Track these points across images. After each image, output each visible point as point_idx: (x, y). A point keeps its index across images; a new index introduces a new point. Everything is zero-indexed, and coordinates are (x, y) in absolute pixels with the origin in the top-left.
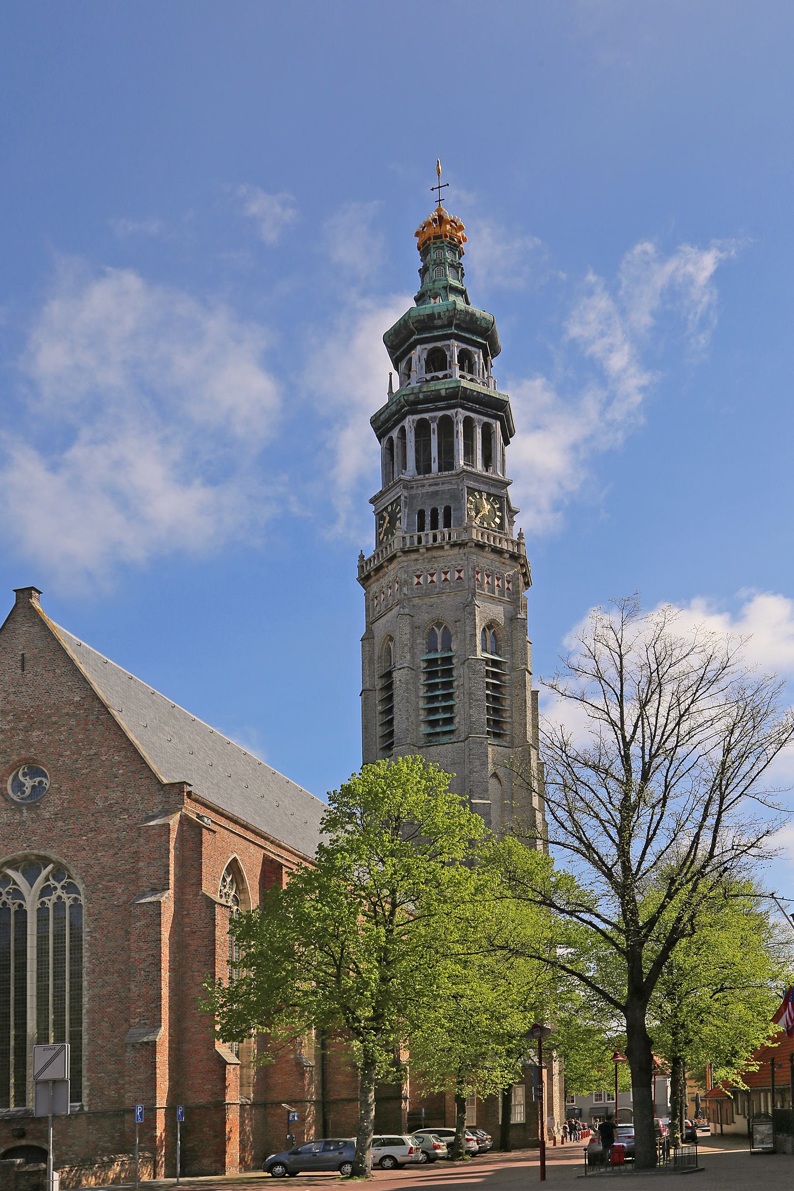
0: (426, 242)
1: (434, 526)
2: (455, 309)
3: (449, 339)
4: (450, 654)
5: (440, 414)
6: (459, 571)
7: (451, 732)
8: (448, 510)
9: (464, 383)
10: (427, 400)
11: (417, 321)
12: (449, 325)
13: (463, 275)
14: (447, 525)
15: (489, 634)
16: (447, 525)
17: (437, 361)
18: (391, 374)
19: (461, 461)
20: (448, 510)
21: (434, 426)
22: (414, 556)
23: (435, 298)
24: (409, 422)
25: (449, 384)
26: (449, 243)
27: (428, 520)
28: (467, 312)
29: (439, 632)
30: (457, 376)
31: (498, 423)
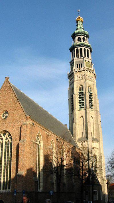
1: (80, 67)
4: (83, 91)
8: (82, 64)
9: (83, 43)
10: (78, 45)
12: (81, 33)
14: (82, 67)
16: (82, 67)
17: (79, 39)
24: (76, 49)
27: (78, 66)
29: (81, 87)
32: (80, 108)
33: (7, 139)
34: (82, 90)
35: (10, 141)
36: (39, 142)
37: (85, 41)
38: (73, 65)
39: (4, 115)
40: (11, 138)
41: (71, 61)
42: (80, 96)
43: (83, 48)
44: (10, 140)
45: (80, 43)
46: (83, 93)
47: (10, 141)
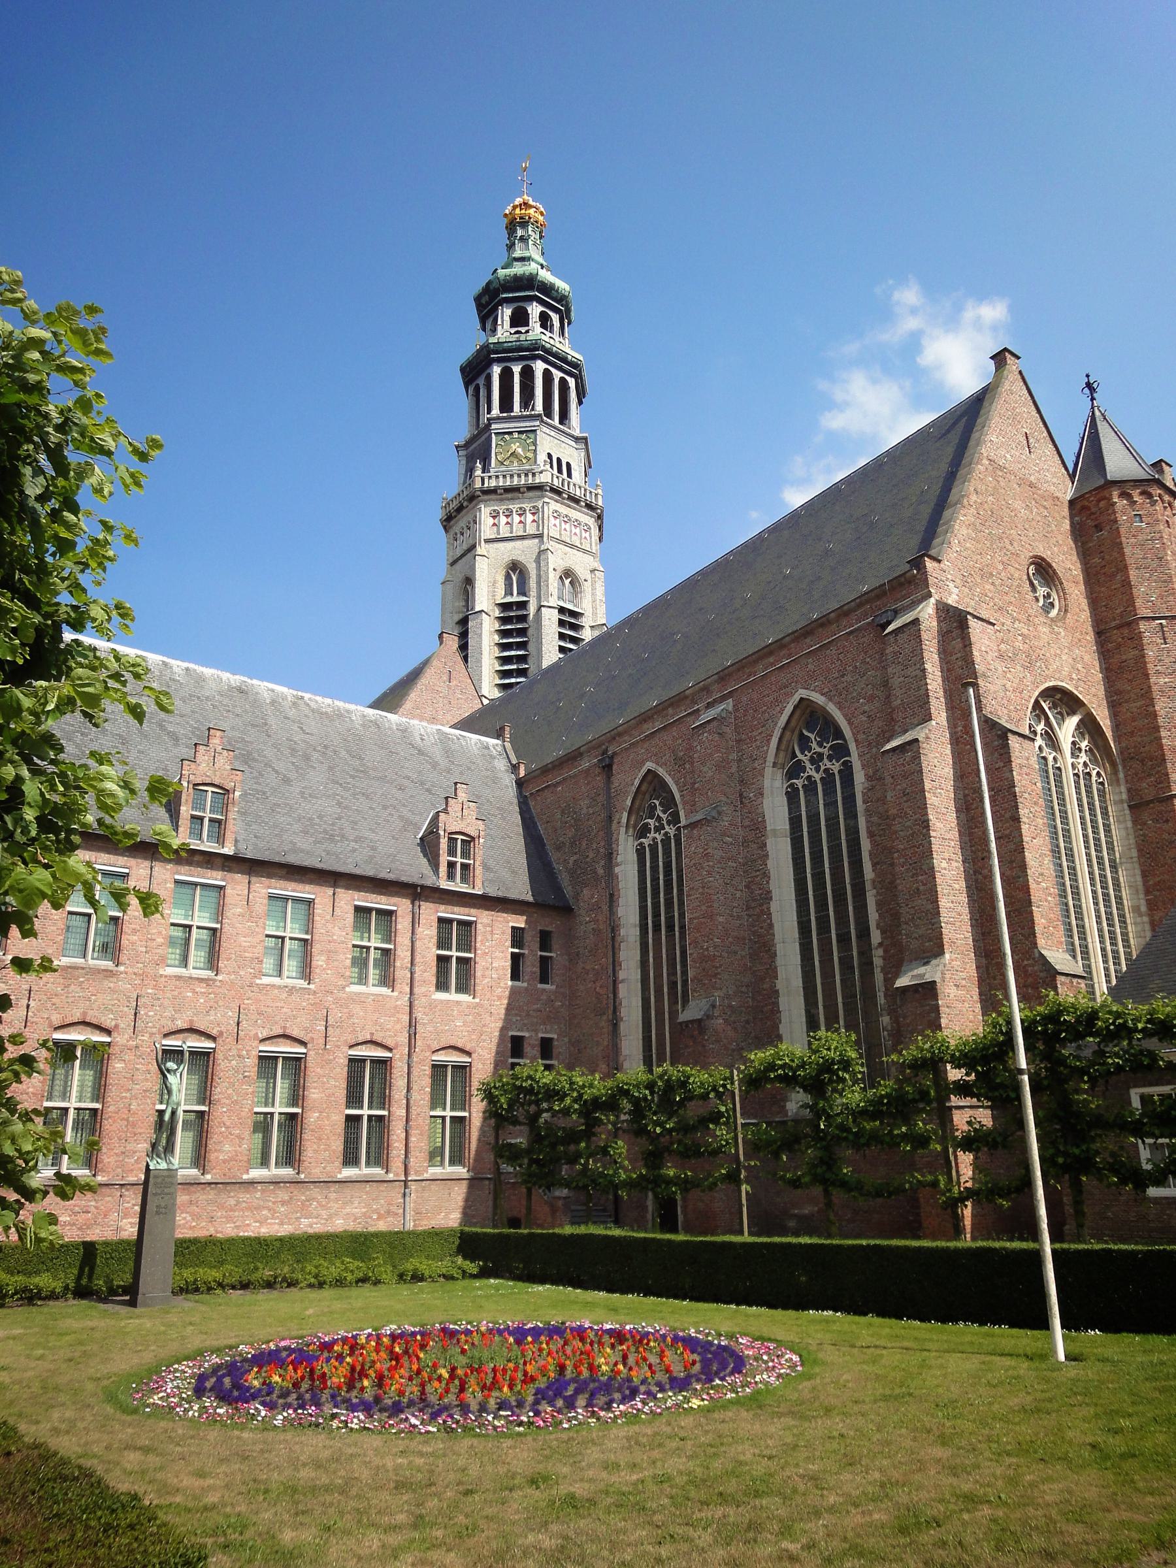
12: (531, 288)
15: (567, 582)
17: (519, 319)
24: (496, 370)
42: (504, 620)
46: (523, 605)
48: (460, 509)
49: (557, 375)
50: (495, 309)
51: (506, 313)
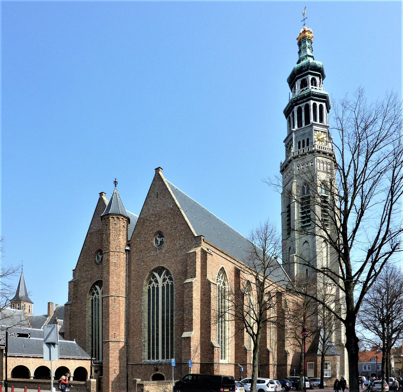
0: (300, 41)
1: (303, 146)
2: (309, 62)
3: (308, 75)
5: (305, 104)
6: (312, 163)
7: (310, 225)
8: (308, 140)
9: (313, 90)
11: (297, 70)
12: (307, 70)
13: (312, 51)
14: (308, 145)
16: (308, 145)
18: (290, 93)
19: (312, 120)
20: (308, 140)
21: (303, 109)
22: (297, 159)
23: (303, 60)
24: (296, 108)
25: (308, 91)
26: (308, 39)
28: (313, 63)
30: (310, 88)
31: (325, 103)
32: (302, 227)
33: (164, 280)
34: (308, 192)
35: (170, 284)
36: (222, 282)
37: (315, 85)
38: (291, 145)
39: (157, 241)
40: (171, 279)
41: (287, 138)
43: (312, 102)
44: (169, 281)
45: (304, 93)
47: (170, 284)
48: (286, 166)
49: (318, 104)
50: (294, 83)
51: (298, 84)
